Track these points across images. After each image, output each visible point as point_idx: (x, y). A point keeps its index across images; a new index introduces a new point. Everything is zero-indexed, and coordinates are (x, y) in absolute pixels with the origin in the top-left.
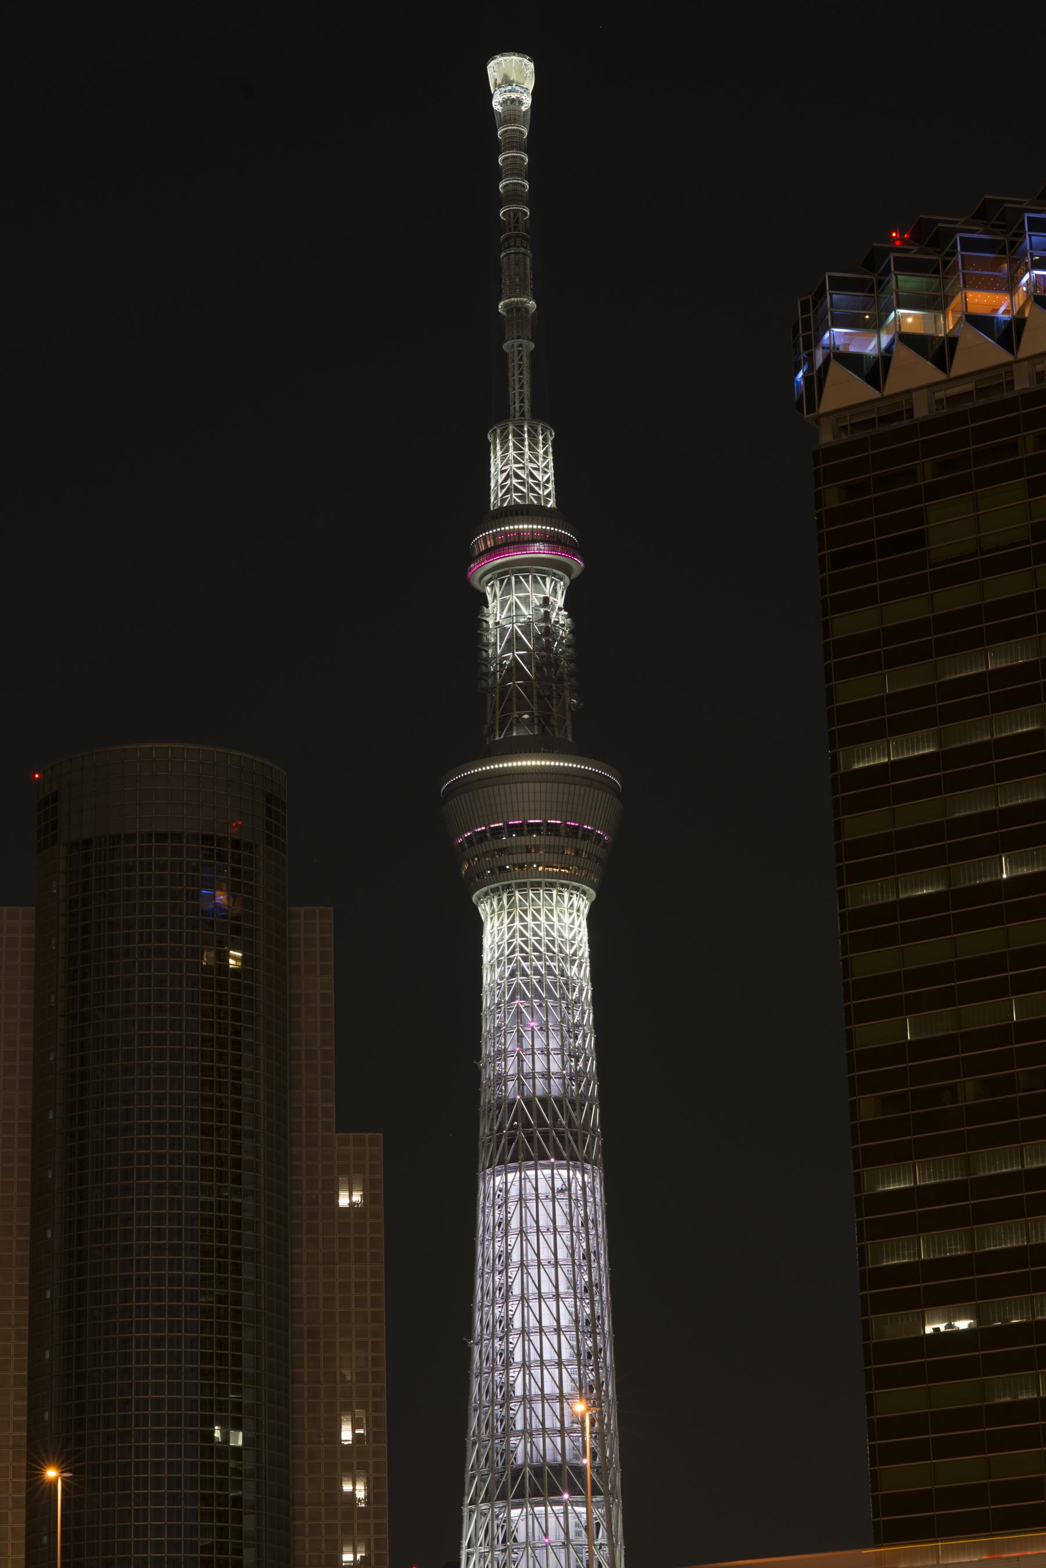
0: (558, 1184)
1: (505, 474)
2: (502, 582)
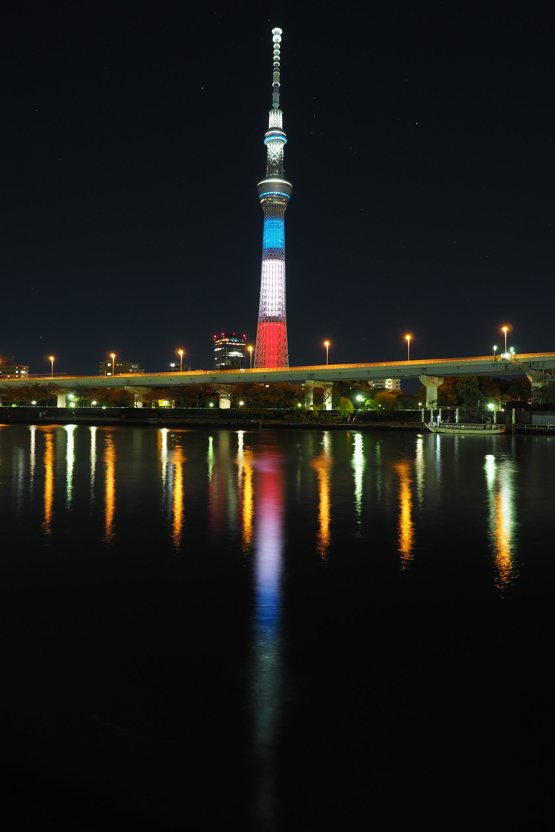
0: (279, 265)
1: (274, 120)
2: (272, 143)
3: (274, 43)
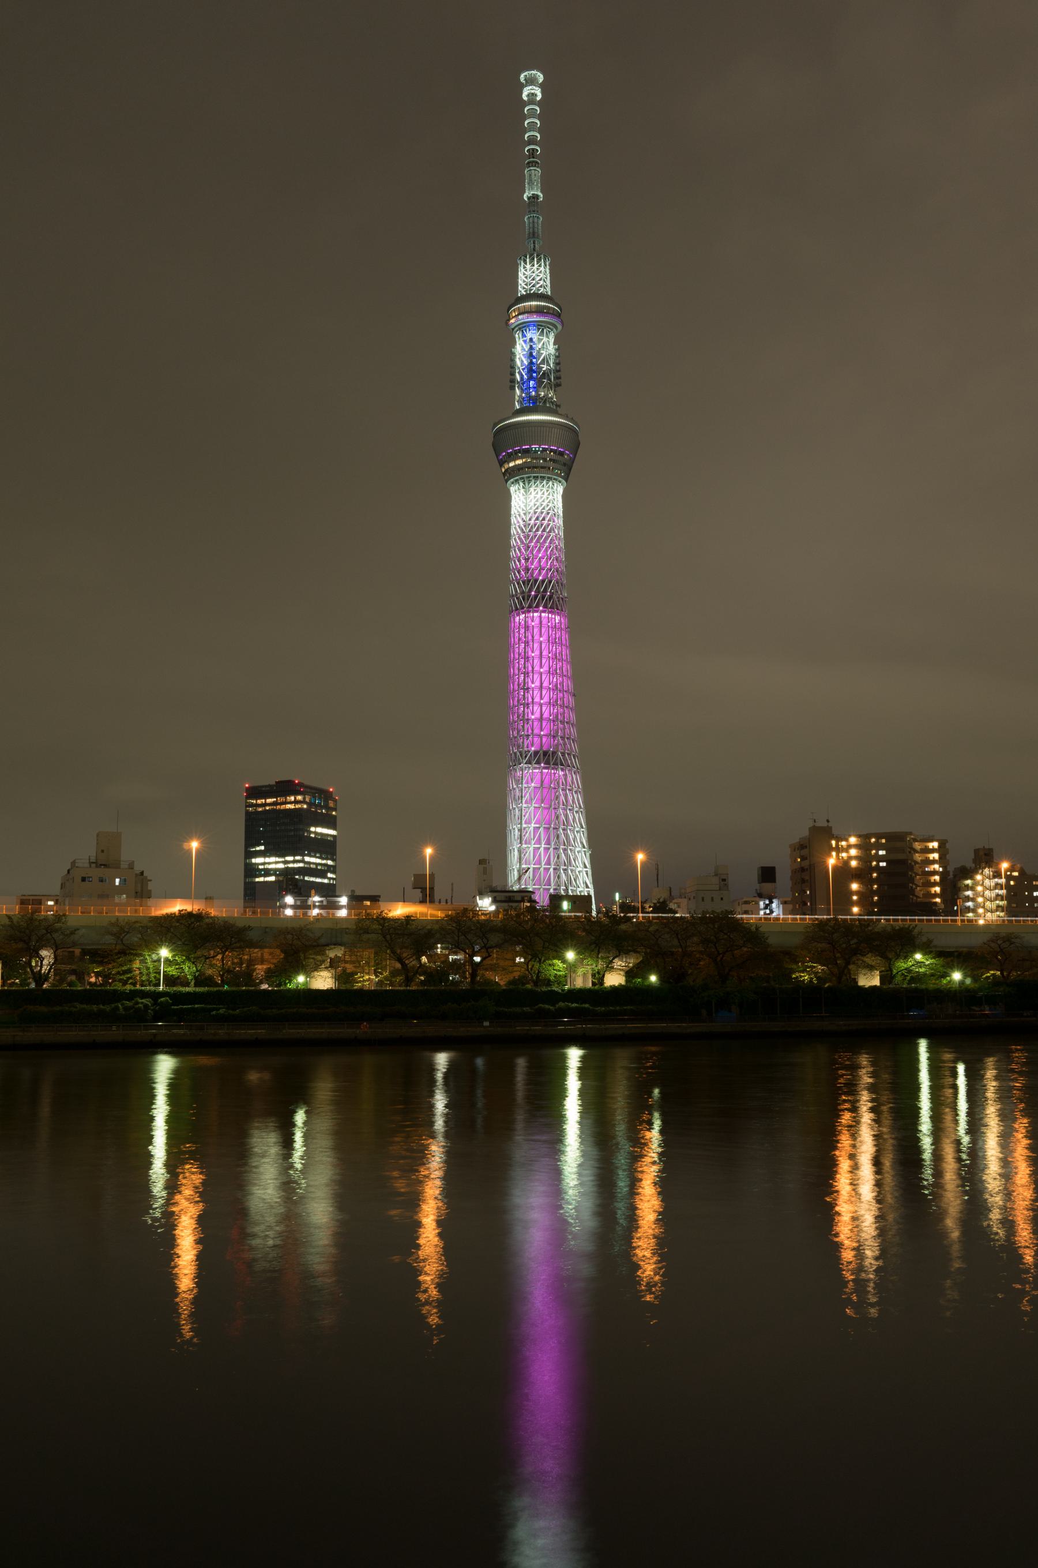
3: (525, 104)
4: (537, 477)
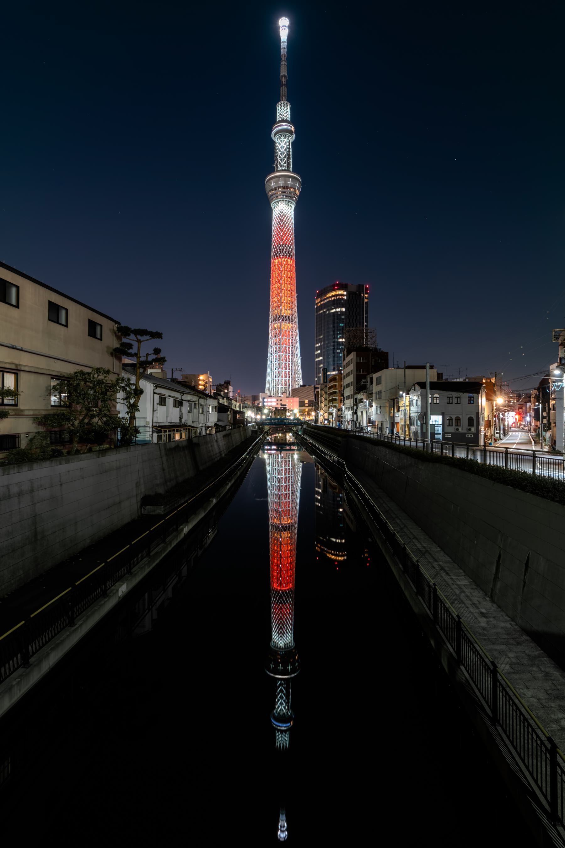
1: (284, 113)
4: (287, 201)
